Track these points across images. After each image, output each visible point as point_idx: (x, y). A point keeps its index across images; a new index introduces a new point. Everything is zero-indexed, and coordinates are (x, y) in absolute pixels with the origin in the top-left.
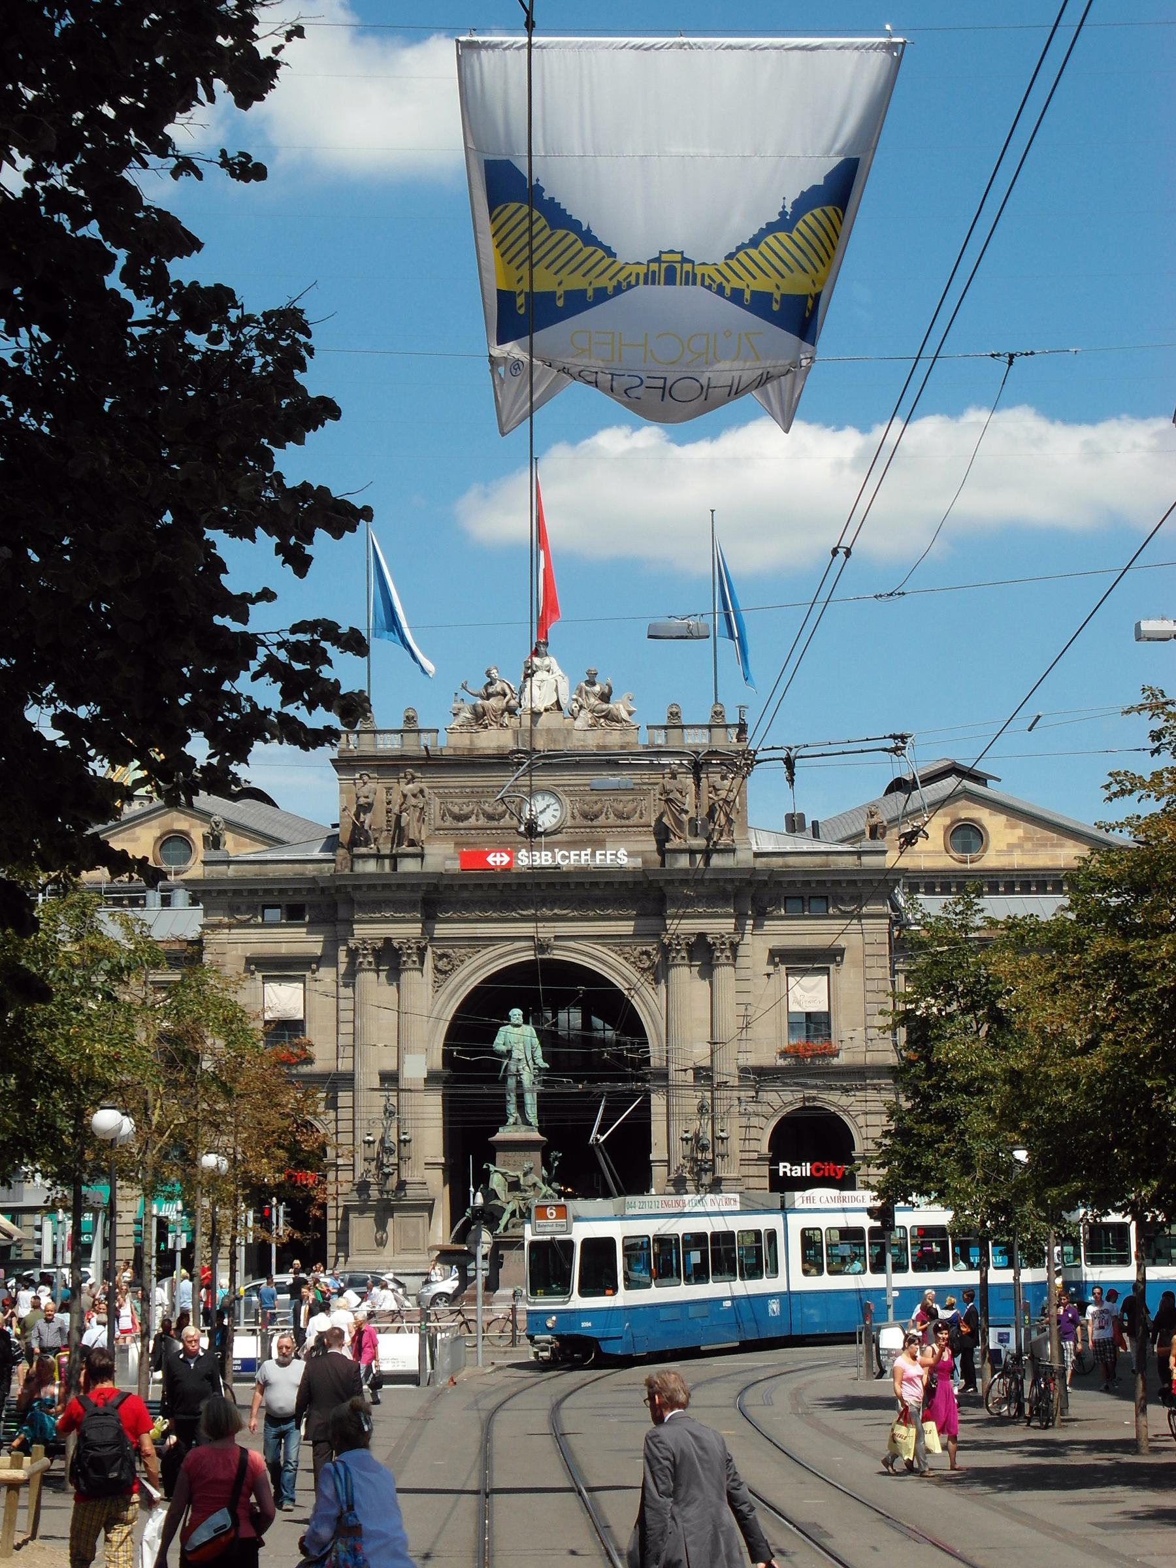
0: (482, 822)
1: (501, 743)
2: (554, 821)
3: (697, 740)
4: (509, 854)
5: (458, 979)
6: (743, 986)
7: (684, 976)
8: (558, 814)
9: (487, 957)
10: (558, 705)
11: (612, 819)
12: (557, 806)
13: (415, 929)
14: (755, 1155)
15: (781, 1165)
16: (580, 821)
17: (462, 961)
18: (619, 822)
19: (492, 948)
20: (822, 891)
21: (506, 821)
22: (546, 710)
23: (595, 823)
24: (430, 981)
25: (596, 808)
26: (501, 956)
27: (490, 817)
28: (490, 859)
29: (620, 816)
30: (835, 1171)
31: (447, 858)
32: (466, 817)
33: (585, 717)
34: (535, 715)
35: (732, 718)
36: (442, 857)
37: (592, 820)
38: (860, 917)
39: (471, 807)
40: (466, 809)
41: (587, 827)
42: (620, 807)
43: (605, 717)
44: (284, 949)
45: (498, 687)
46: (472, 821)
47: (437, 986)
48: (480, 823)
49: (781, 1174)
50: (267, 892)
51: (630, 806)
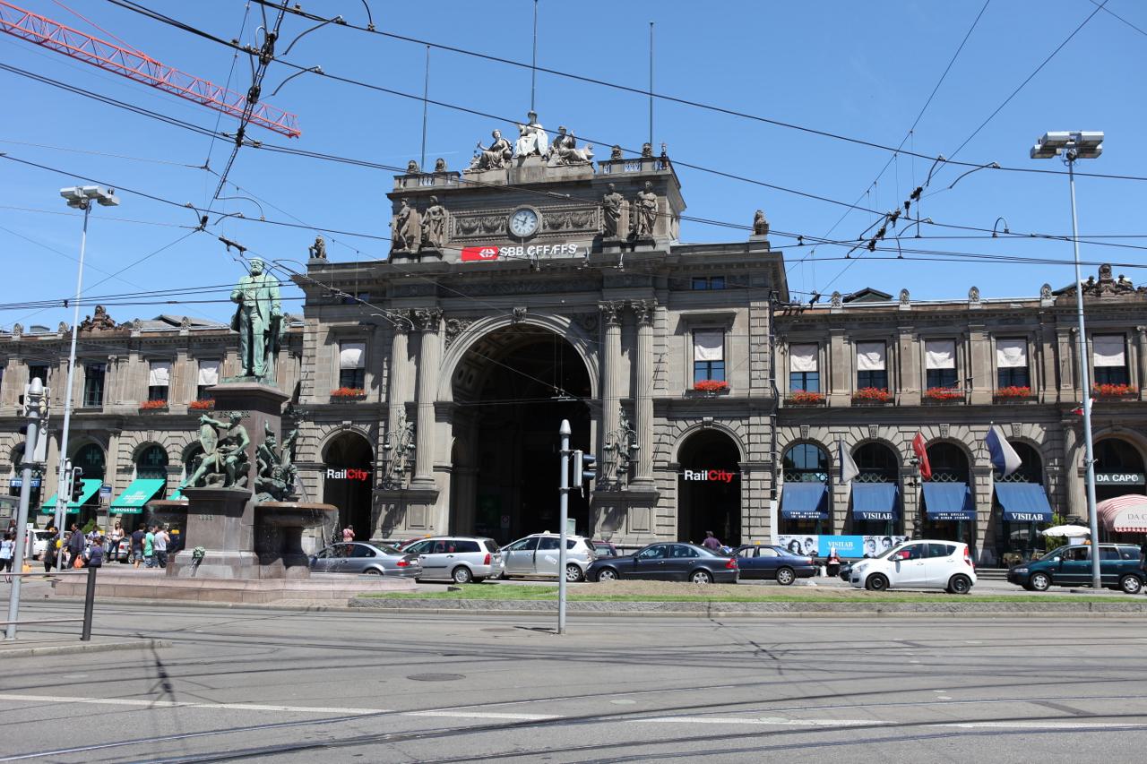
0: (483, 233)
1: (498, 179)
2: (531, 229)
3: (631, 170)
4: (495, 250)
6: (659, 341)
10: (537, 152)
11: (571, 228)
14: (666, 464)
15: (686, 472)
16: (548, 229)
18: (576, 229)
21: (498, 232)
22: (529, 155)
23: (560, 230)
24: (443, 341)
25: (561, 220)
27: (488, 229)
29: (576, 225)
30: (726, 477)
31: (457, 257)
32: (473, 230)
33: (556, 159)
34: (522, 157)
35: (656, 153)
36: (453, 256)
40: (473, 225)
41: (555, 231)
45: (500, 143)
47: (448, 344)
48: (483, 233)
49: (686, 478)
51: (583, 218)
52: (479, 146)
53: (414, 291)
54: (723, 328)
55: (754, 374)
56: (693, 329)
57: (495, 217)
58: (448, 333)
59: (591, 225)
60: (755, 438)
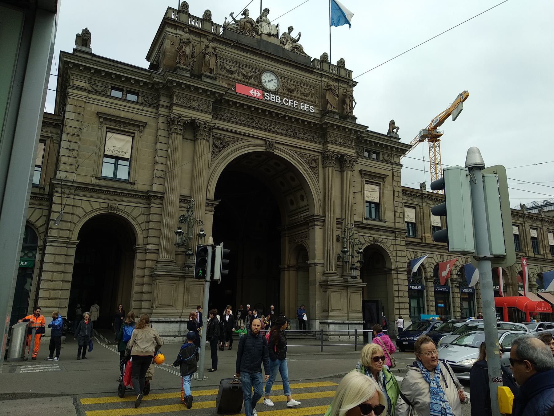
2: (274, 88)
5: (225, 153)
7: (333, 173)
8: (276, 85)
9: (241, 145)
10: (277, 36)
12: (276, 81)
13: (208, 118)
17: (228, 145)
19: (244, 141)
20: (378, 150)
22: (273, 35)
23: (292, 94)
25: (293, 87)
26: (249, 146)
28: (251, 92)
37: (291, 92)
38: (392, 164)
39: (235, 69)
40: (233, 69)
42: (303, 90)
43: (296, 48)
44: (123, 114)
46: (236, 76)
47: (214, 154)
48: (239, 78)
50: (118, 77)
51: (307, 92)
52: (231, 15)
53: (194, 104)
54: (380, 184)
55: (397, 214)
56: (366, 181)
58: (214, 144)
59: (312, 97)
60: (399, 254)
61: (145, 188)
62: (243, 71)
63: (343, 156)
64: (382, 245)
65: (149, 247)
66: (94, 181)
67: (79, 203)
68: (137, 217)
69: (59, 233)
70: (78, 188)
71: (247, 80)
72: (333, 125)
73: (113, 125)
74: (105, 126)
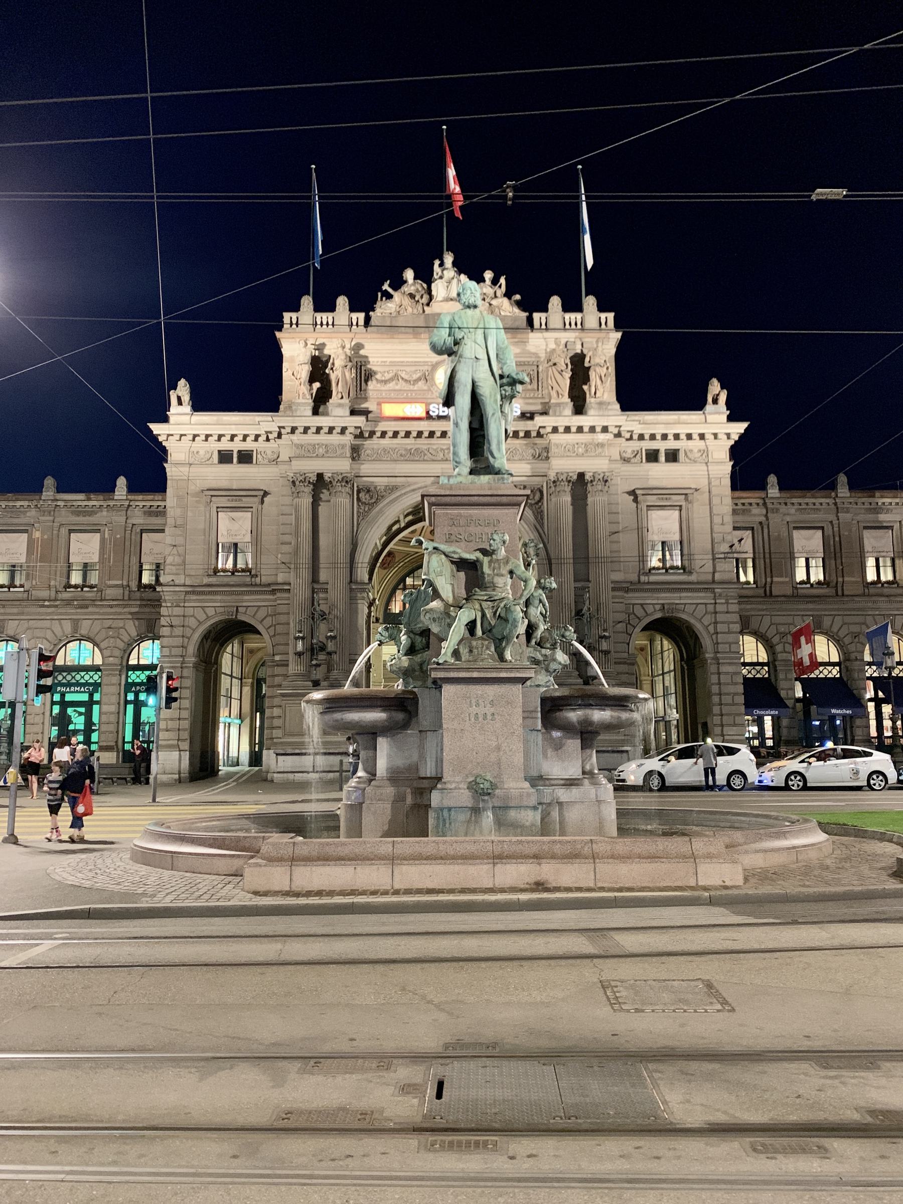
27: (406, 381)
39: (391, 375)
48: (397, 388)
57: (414, 368)
61: (270, 580)
62: (403, 375)
63: (581, 475)
64: (684, 616)
65: (277, 658)
66: (206, 580)
67: (190, 611)
68: (263, 620)
69: (170, 651)
70: (187, 593)
71: (411, 387)
72: (555, 430)
73: (223, 502)
74: (215, 506)
